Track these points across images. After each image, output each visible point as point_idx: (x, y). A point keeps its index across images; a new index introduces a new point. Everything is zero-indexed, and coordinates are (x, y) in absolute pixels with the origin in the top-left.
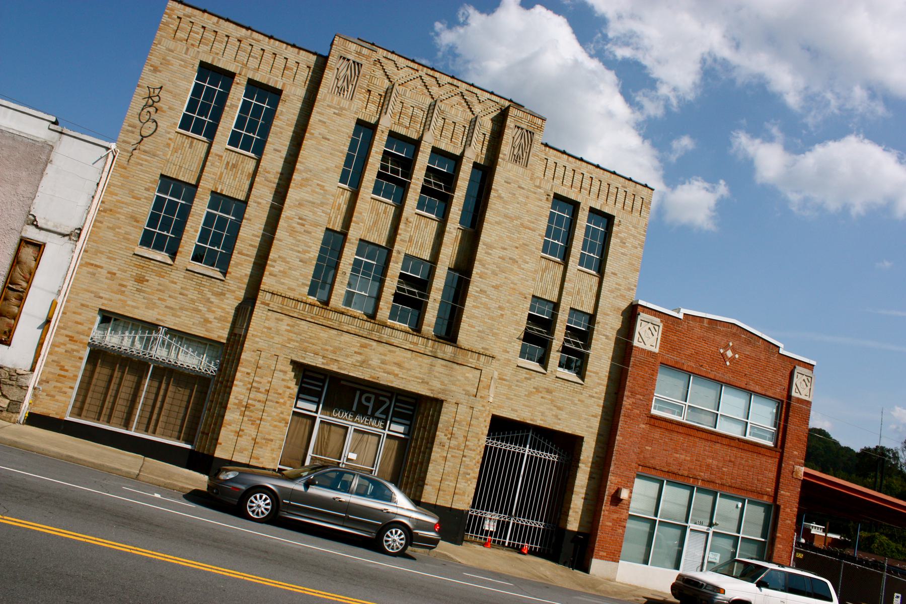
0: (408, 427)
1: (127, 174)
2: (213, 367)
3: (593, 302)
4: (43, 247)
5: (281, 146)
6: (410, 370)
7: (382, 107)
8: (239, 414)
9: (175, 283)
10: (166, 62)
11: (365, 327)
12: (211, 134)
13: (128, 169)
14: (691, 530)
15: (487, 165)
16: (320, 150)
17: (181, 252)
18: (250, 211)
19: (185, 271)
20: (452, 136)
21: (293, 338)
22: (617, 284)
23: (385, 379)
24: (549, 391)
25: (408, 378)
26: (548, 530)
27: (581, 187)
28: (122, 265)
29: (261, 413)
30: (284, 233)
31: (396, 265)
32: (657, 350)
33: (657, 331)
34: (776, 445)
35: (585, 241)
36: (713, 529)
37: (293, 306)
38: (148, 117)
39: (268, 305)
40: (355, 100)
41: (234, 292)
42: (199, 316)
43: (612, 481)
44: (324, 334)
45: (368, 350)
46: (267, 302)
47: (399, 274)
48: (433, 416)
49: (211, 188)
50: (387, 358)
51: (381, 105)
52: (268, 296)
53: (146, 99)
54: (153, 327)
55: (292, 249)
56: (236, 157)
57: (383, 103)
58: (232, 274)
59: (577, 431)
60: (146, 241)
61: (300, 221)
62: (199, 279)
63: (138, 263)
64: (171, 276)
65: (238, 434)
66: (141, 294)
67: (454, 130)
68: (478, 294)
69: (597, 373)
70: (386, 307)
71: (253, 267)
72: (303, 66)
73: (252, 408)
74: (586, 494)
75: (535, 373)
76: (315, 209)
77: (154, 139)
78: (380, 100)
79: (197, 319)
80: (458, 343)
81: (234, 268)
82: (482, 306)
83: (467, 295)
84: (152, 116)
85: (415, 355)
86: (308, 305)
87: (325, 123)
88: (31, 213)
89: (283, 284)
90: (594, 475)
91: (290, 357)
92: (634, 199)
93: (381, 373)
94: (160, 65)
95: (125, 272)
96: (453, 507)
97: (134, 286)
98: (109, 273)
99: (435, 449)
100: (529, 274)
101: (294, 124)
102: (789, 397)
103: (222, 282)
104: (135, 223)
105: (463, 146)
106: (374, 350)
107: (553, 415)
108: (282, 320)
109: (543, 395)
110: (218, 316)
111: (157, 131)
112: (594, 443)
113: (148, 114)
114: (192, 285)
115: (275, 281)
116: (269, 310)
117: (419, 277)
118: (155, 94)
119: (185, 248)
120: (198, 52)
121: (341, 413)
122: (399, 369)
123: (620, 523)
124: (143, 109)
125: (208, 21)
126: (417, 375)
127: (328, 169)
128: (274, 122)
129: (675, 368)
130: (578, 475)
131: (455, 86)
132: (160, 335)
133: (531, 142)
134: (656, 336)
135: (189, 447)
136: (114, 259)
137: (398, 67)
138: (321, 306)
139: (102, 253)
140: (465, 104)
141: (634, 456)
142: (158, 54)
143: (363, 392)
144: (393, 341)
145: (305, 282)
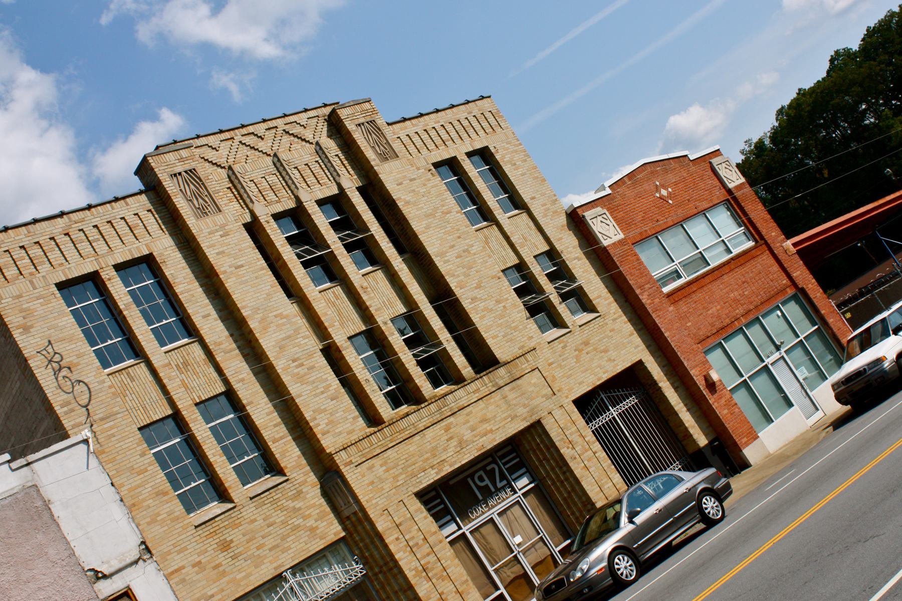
0: (528, 474)
1: (110, 457)
2: (358, 567)
3: (541, 237)
4: (129, 592)
5: (205, 309)
6: (495, 416)
7: (242, 198)
8: (425, 582)
9: (255, 520)
10: (27, 313)
12: (137, 351)
13: (106, 450)
14: (771, 364)
15: (365, 183)
16: (246, 282)
19: (251, 502)
20: (317, 179)
21: (396, 473)
22: (543, 205)
24: (586, 343)
25: (501, 425)
26: (685, 465)
27: (443, 141)
28: (196, 547)
29: (439, 564)
31: (394, 337)
32: (621, 236)
34: (756, 241)
36: (783, 350)
38: (69, 383)
39: (351, 462)
40: (223, 208)
41: (305, 482)
42: (303, 532)
43: (696, 374)
44: (412, 447)
45: (454, 429)
46: (348, 460)
47: (403, 343)
48: (542, 441)
50: (472, 423)
51: (239, 198)
52: (343, 453)
53: (50, 366)
54: (279, 579)
55: (316, 395)
57: (239, 194)
58: (288, 466)
61: (296, 363)
62: (269, 497)
63: (208, 533)
64: (246, 517)
66: (240, 558)
67: (312, 171)
68: (473, 305)
69: (599, 297)
70: (423, 382)
71: (297, 444)
72: (143, 214)
73: (429, 566)
74: (686, 405)
76: (296, 341)
77: (97, 400)
78: (233, 193)
79: (304, 535)
81: (285, 460)
83: (467, 313)
84: (71, 378)
85: (486, 400)
87: (223, 252)
88: (86, 569)
89: (340, 433)
90: (676, 385)
91: (410, 493)
92: (485, 118)
93: (481, 440)
94: (25, 321)
95: (206, 551)
97: (227, 557)
98: (194, 566)
99: (572, 465)
100: (482, 254)
101: (194, 278)
102: (729, 191)
103: (288, 482)
104: (166, 498)
105: (333, 181)
106: (457, 425)
107: (607, 361)
110: (316, 516)
111: (92, 390)
112: (651, 357)
113: (67, 380)
114: (270, 508)
115: (332, 437)
117: (412, 334)
118: (52, 354)
120: (43, 277)
121: (476, 511)
122: (487, 424)
123: (731, 405)
124: (57, 379)
125: (21, 237)
127: (268, 295)
128: (177, 291)
129: (643, 239)
130: (666, 394)
131: (273, 128)
134: (611, 225)
136: (186, 549)
137: (215, 148)
138: (376, 429)
139: (169, 553)
140: (296, 140)
141: (689, 340)
142: (10, 311)
143: (472, 476)
145: (353, 415)
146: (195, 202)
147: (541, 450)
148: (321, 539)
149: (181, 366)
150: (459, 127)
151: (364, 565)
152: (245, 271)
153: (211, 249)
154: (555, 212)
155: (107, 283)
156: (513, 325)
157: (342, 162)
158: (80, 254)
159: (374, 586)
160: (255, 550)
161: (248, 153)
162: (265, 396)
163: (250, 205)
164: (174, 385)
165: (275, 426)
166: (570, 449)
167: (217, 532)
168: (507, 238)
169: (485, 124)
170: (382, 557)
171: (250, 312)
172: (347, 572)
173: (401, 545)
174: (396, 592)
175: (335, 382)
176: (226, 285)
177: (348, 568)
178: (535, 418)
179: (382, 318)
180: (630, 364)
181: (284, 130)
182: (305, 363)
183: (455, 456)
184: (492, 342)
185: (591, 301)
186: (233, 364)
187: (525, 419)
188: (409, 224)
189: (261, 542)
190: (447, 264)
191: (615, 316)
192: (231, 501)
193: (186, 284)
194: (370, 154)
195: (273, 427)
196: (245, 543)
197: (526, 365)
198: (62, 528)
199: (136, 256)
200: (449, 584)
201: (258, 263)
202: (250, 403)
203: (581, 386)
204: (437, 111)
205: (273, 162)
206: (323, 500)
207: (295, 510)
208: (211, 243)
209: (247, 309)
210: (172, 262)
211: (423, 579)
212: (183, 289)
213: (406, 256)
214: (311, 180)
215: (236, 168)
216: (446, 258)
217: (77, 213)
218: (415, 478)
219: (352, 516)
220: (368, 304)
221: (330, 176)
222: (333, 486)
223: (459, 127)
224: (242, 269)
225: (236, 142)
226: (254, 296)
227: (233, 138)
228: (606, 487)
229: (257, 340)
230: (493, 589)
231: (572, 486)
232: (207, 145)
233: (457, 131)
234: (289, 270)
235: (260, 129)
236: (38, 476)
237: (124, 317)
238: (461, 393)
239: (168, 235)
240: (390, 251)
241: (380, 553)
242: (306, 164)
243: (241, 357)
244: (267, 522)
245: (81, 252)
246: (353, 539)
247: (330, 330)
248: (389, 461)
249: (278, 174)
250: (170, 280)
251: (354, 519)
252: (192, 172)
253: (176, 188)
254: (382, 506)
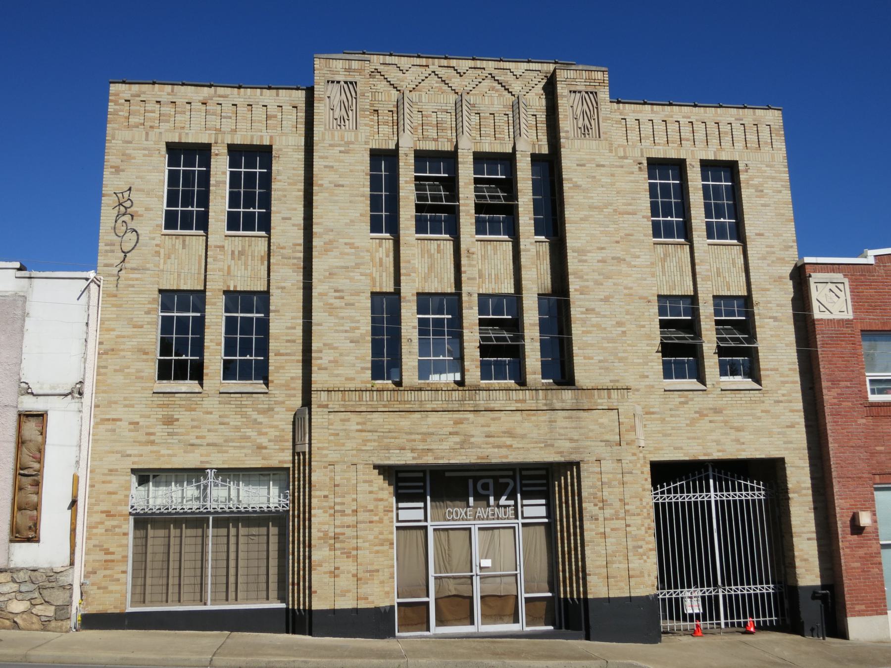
9: (211, 413)
11: (454, 399)
12: (203, 223)
17: (207, 374)
18: (275, 301)
19: (218, 395)
22: (767, 246)
23: (497, 456)
24: (717, 411)
30: (321, 314)
31: (470, 311)
32: (850, 315)
33: (843, 289)
35: (707, 207)
37: (357, 399)
39: (326, 406)
41: (283, 402)
44: (405, 422)
45: (466, 426)
47: (478, 321)
49: (221, 287)
52: (324, 395)
53: (117, 208)
55: (337, 331)
56: (240, 242)
58: (275, 382)
60: (164, 372)
61: (337, 294)
63: (162, 403)
64: (204, 406)
65: (334, 573)
66: (175, 437)
68: (584, 316)
70: (474, 366)
75: (691, 392)
80: (576, 384)
81: (276, 374)
82: (595, 329)
86: (375, 393)
87: (332, 167)
89: (337, 376)
91: (371, 462)
96: (633, 595)
97: (164, 430)
98: (130, 423)
103: (265, 395)
104: (145, 357)
106: (473, 423)
107: (732, 441)
108: (348, 420)
109: (711, 419)
110: (273, 438)
113: (124, 224)
118: (126, 199)
119: (211, 368)
120: (161, 133)
124: (116, 221)
125: (162, 93)
127: (352, 221)
133: (597, 105)
136: (132, 406)
139: (116, 403)
143: (476, 479)
144: (492, 405)
145: (363, 365)
148: (263, 459)
167: (170, 406)
173: (325, 504)
178: (574, 457)
179: (470, 288)
190: (581, 264)
191: (781, 398)
197: (606, 401)
198: (25, 341)
202: (276, 311)
218: (387, 452)
221: (511, 133)
227: (427, 66)
236: (32, 291)
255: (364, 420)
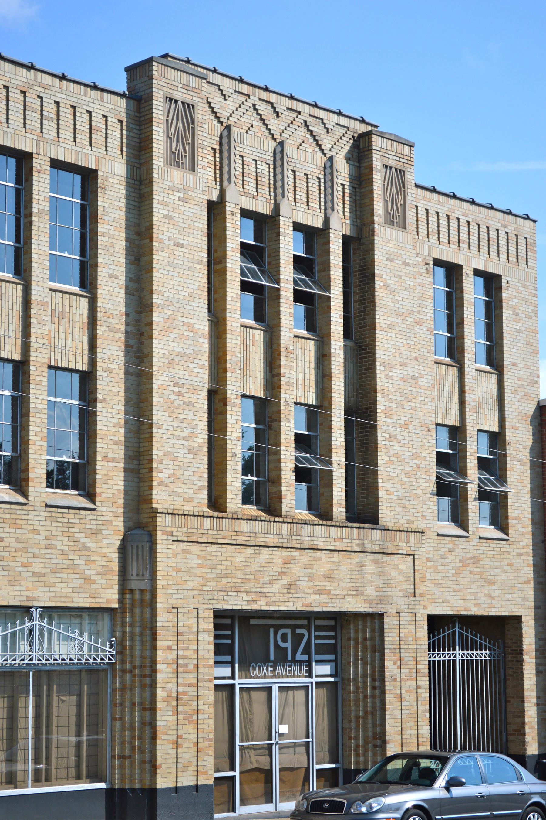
0: (334, 664)
3: (496, 413)
5: (116, 268)
9: (37, 532)
15: (355, 236)
16: (176, 266)
19: (44, 509)
20: (308, 198)
21: (209, 575)
22: (519, 379)
24: (476, 561)
25: (341, 593)
29: (195, 703)
31: (288, 424)
37: (199, 527)
39: (171, 533)
40: (199, 169)
42: (77, 576)
46: (169, 529)
47: (293, 438)
48: (372, 639)
50: (314, 571)
51: (218, 168)
55: (176, 437)
58: (104, 495)
59: (514, 610)
61: (176, 389)
62: (65, 515)
64: (30, 522)
67: (308, 186)
68: (387, 443)
69: (518, 519)
73: (185, 698)
74: (538, 697)
75: (457, 539)
76: (190, 365)
78: (215, 157)
80: (380, 523)
81: (104, 486)
86: (215, 519)
89: (178, 494)
90: (541, 668)
91: (211, 606)
92: (517, 242)
93: (313, 596)
100: (426, 392)
103: (93, 513)
105: (323, 211)
107: (486, 595)
109: (471, 569)
110: (100, 568)
112: (533, 621)
114: (59, 529)
115: (166, 493)
116: (174, 541)
121: (259, 669)
122: (328, 584)
126: (349, 585)
128: (99, 229)
130: (525, 672)
131: (296, 111)
132: (35, 622)
135: (102, 785)
137: (224, 96)
140: (311, 140)
143: (277, 628)
145: (200, 483)
146: (174, 144)
147: (365, 647)
149: (57, 315)
150: (484, 235)
151: (116, 654)
152: (181, 254)
153: (161, 207)
154: (528, 395)
155: (34, 173)
156: (415, 492)
157: (344, 196)
158: (25, 124)
159: (113, 682)
160: (19, 564)
161: (255, 123)
162: (123, 403)
163: (225, 183)
164: (39, 331)
165: (115, 443)
166: (396, 667)
168: (462, 391)
169: (512, 249)
170: (143, 657)
171: (161, 302)
172: (97, 649)
173: (170, 657)
174: (134, 704)
175: (203, 437)
176: (155, 257)
177: (99, 646)
179: (288, 396)
180: (506, 614)
181: (305, 121)
182: (185, 395)
183: (277, 595)
184: (384, 496)
185: (507, 518)
186: (110, 347)
187: (369, 603)
188: (374, 310)
189: (30, 560)
190: (387, 380)
191: (523, 551)
192: (26, 496)
193: (112, 228)
194: (379, 206)
195: (111, 442)
196: (14, 550)
197: (405, 544)
199: (80, 164)
200: (192, 731)
201: (200, 254)
202: (104, 401)
203: (444, 604)
204: (473, 202)
205: (275, 150)
206: (116, 555)
207: (84, 548)
208: (166, 199)
209: (160, 297)
210: (112, 193)
211: (170, 708)
212: (106, 231)
213: (350, 343)
214: (301, 195)
215: (235, 131)
216: (390, 373)
217: (47, 76)
218: (225, 593)
219: (137, 592)
220: (282, 371)
221: (322, 204)
222: (137, 547)
223: (484, 235)
224: (180, 249)
225: (249, 103)
226: (176, 287)
228: (409, 732)
229: (151, 337)
230: (227, 766)
231: (374, 708)
232: (219, 86)
233: (479, 238)
234: (225, 281)
235: (283, 104)
237: (31, 223)
238: (322, 531)
239: (124, 161)
240: (337, 328)
241: (142, 651)
242: (307, 175)
243: (122, 345)
244: (48, 542)
245: (27, 121)
246: (123, 617)
247: (228, 374)
248: (209, 558)
249: (272, 166)
250: (99, 212)
251: (137, 596)
252: (189, 107)
253: (163, 115)
254: (175, 601)
255: (204, 553)
